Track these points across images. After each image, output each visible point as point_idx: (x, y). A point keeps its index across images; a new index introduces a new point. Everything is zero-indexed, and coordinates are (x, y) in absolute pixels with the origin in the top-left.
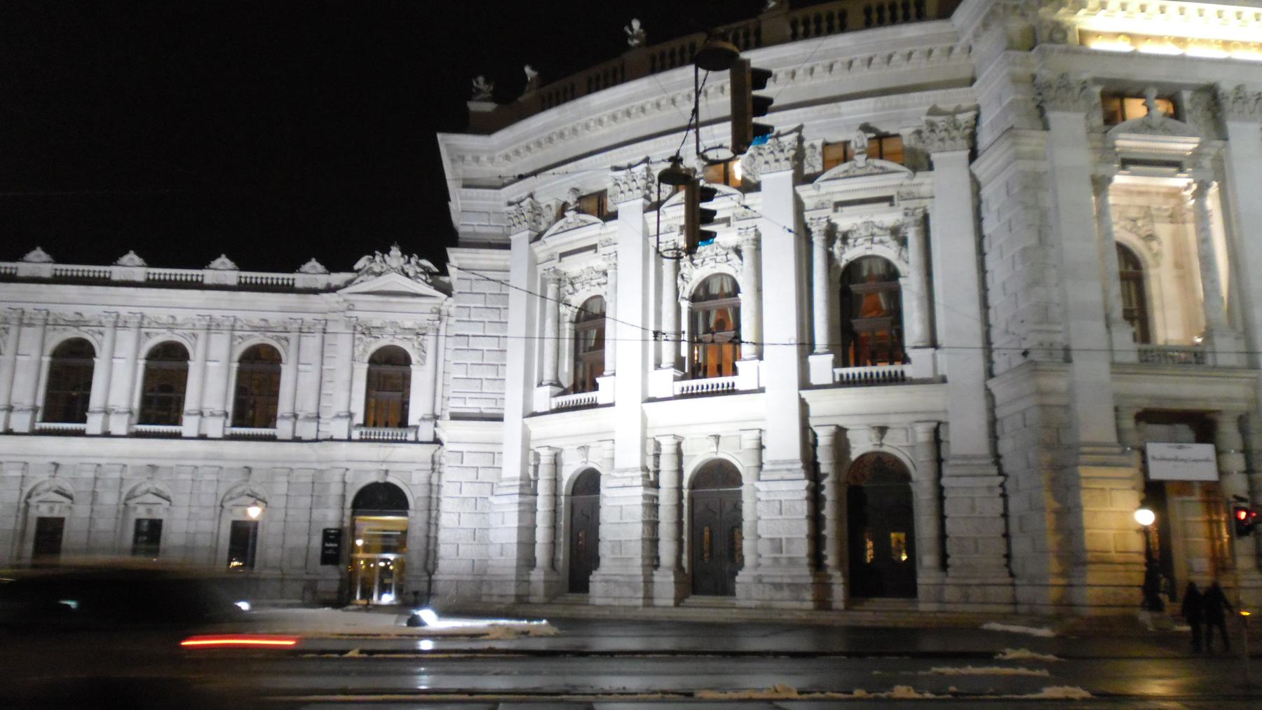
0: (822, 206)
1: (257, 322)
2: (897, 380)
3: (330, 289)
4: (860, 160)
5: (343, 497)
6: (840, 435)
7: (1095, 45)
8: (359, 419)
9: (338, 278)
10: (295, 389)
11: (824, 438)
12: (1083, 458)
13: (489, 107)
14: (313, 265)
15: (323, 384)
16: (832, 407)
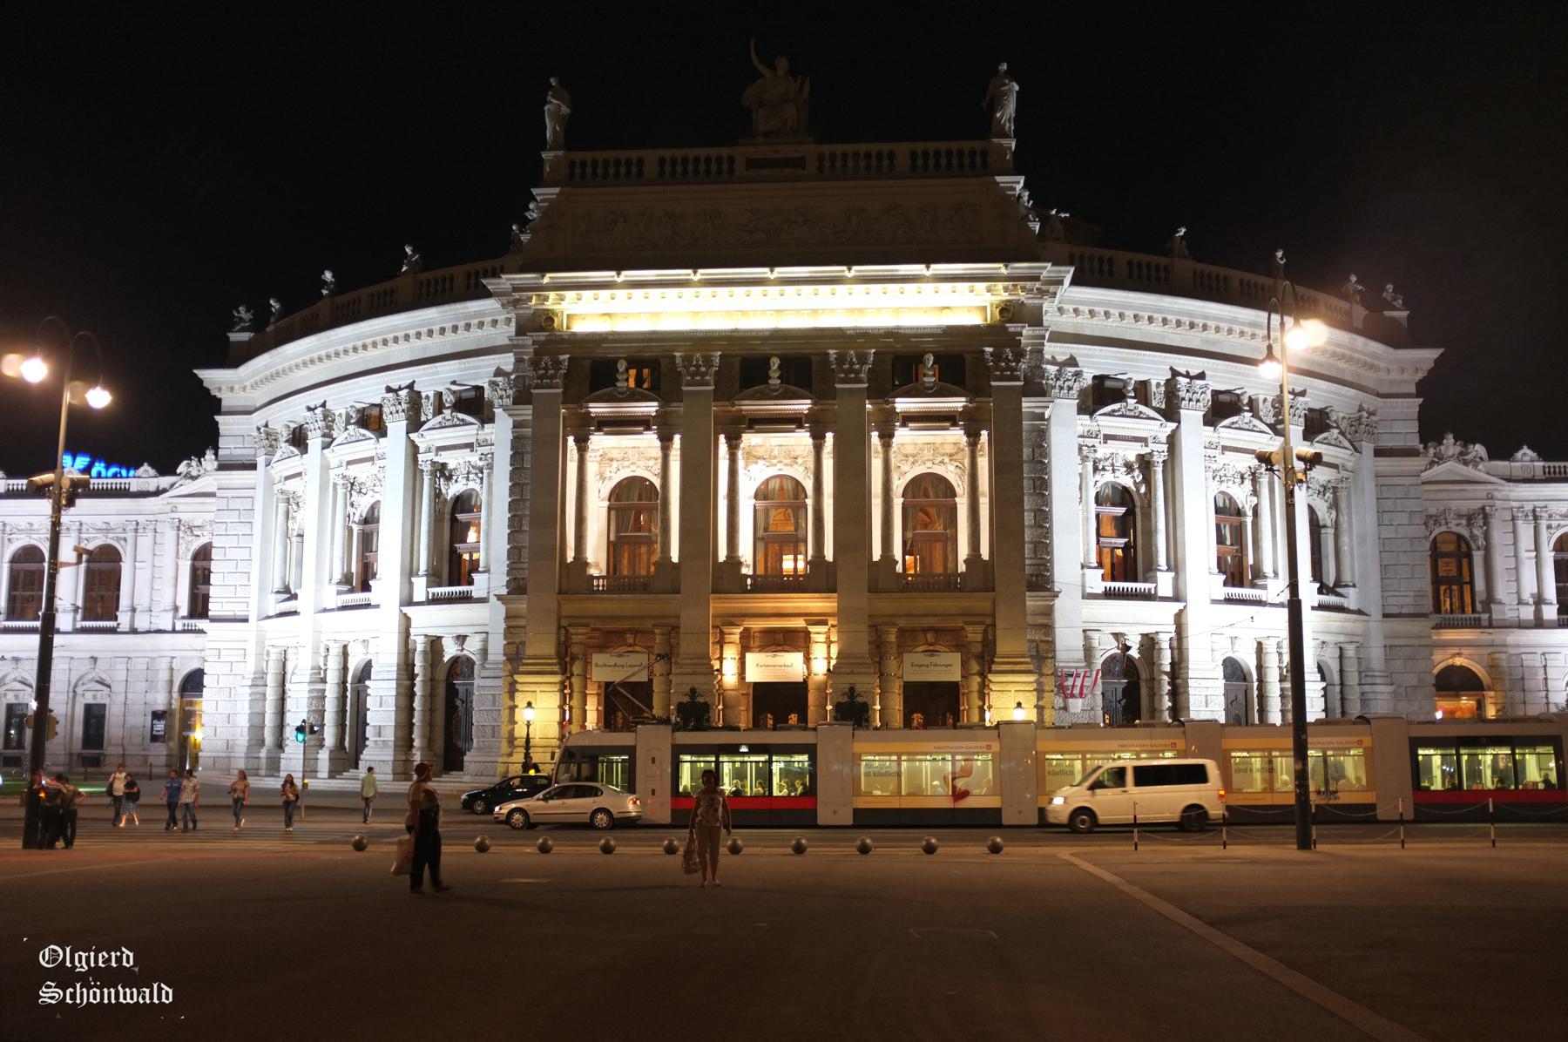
0: (429, 450)
1: (100, 525)
2: (466, 599)
3: (158, 492)
4: (447, 412)
5: (171, 682)
6: (435, 644)
7: (579, 327)
8: (184, 611)
9: (165, 481)
10: (134, 584)
11: (420, 644)
12: (522, 668)
13: (245, 336)
14: (146, 469)
15: (152, 584)
16: (429, 621)
